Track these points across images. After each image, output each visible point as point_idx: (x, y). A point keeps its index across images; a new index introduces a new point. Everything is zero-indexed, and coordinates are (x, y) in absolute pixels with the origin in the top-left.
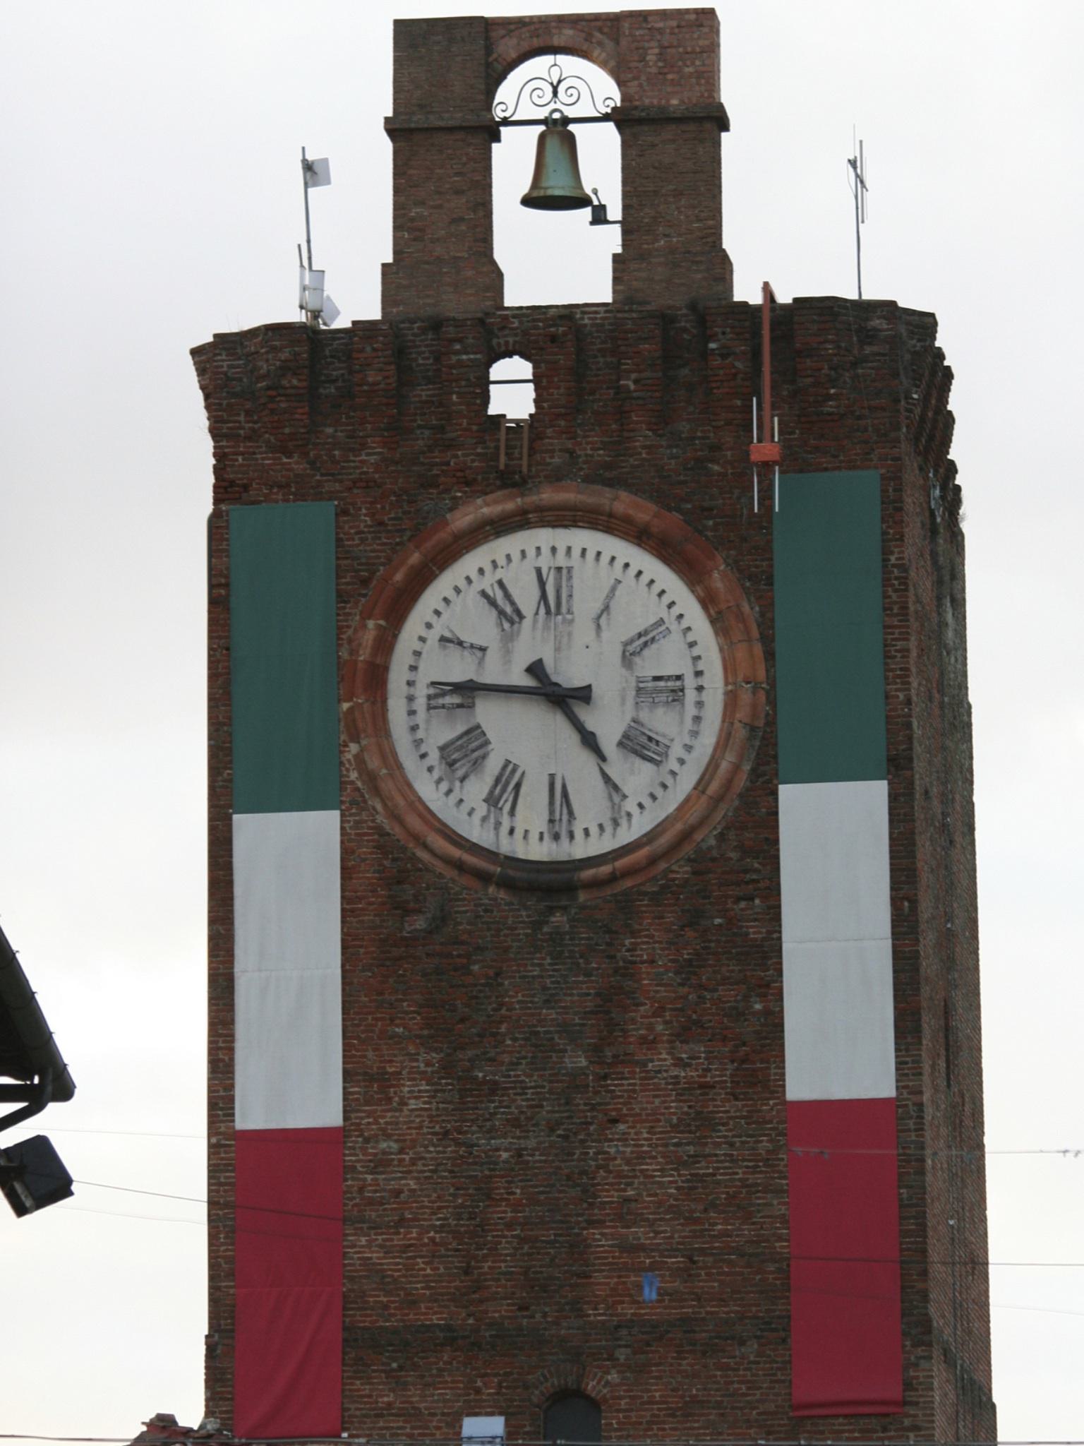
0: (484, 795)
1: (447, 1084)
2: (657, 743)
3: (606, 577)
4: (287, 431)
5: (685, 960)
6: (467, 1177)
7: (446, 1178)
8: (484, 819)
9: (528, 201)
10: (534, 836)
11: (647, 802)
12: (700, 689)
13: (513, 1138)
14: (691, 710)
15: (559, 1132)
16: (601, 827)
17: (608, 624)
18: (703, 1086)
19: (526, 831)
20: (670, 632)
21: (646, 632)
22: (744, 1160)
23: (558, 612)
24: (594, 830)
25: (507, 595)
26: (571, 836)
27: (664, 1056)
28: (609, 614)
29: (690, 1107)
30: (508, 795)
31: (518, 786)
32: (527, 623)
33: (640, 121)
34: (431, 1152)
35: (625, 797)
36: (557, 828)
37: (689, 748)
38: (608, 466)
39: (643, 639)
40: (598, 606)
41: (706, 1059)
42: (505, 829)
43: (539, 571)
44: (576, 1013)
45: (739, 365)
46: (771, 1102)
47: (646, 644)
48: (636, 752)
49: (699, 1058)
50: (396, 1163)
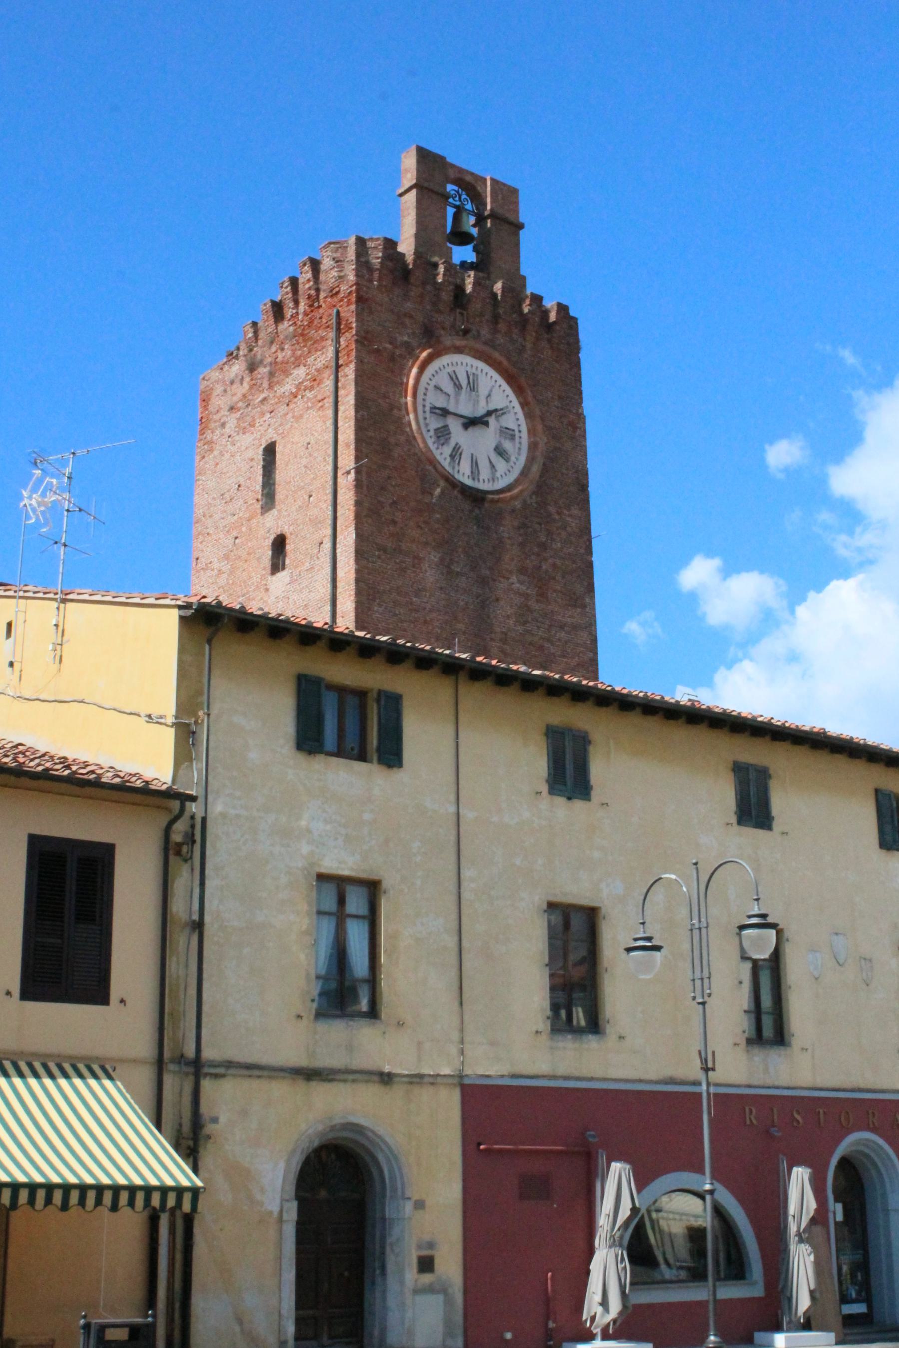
2: (507, 454)
8: (449, 464)
11: (504, 475)
12: (520, 437)
14: (518, 445)
16: (489, 480)
18: (527, 594)
21: (502, 410)
23: (474, 391)
25: (457, 378)
26: (479, 480)
30: (458, 457)
31: (461, 454)
39: (502, 412)
40: (487, 393)
43: (467, 372)
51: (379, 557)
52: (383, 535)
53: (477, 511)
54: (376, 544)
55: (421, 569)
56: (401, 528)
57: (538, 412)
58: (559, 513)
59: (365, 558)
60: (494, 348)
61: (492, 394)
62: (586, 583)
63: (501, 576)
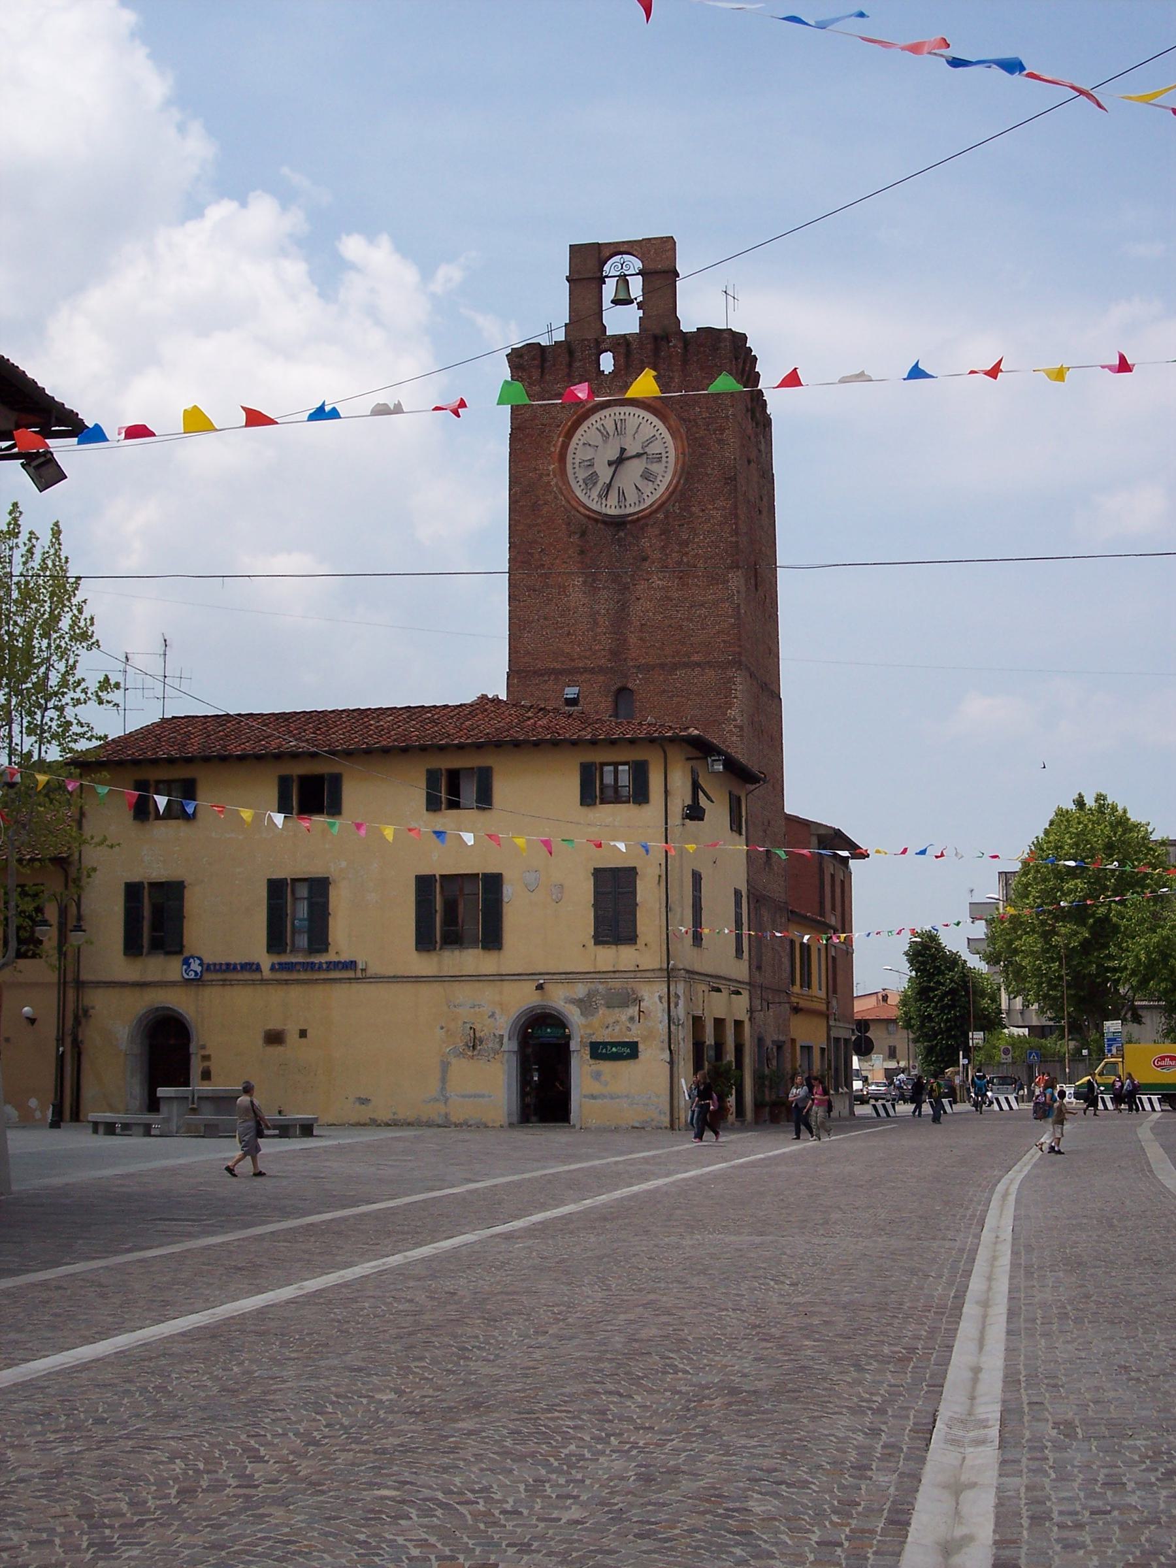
3: (637, 421)
9: (613, 302)
10: (613, 507)
14: (664, 464)
32: (611, 437)
33: (648, 273)
42: (604, 505)
51: (529, 596)
58: (703, 510)
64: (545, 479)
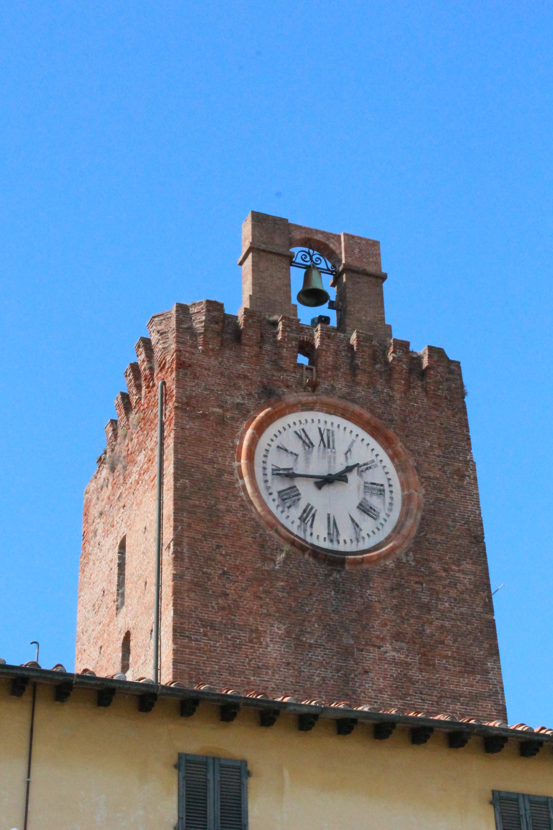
0: (299, 515)
1: (288, 640)
2: (374, 510)
3: (349, 438)
4: (210, 346)
5: (395, 605)
6: (300, 686)
7: (289, 684)
8: (299, 527)
11: (371, 534)
12: (391, 492)
13: (321, 671)
14: (388, 500)
15: (342, 672)
16: (351, 540)
17: (351, 457)
18: (406, 663)
19: (318, 536)
20: (377, 466)
21: (367, 464)
22: (427, 700)
23: (329, 447)
24: (348, 541)
25: (307, 436)
26: (338, 542)
27: (388, 645)
28: (351, 453)
29: (401, 671)
30: (310, 518)
31: (314, 516)
32: (316, 449)
34: (282, 671)
35: (361, 530)
36: (332, 537)
37: (388, 516)
38: (349, 394)
39: (366, 467)
40: (346, 449)
41: (407, 650)
42: (308, 533)
43: (320, 429)
44: (348, 619)
45: (404, 366)
46: (437, 675)
47: (367, 469)
48: (365, 512)
49: (404, 649)
50: (264, 673)
51: (205, 635)
52: (210, 609)
53: (335, 575)
54: (201, 620)
55: (261, 644)
56: (235, 601)
57: (412, 462)
58: (445, 570)
59: (187, 637)
60: (354, 401)
61: (352, 449)
62: (486, 646)
63: (368, 645)
64: (226, 477)
